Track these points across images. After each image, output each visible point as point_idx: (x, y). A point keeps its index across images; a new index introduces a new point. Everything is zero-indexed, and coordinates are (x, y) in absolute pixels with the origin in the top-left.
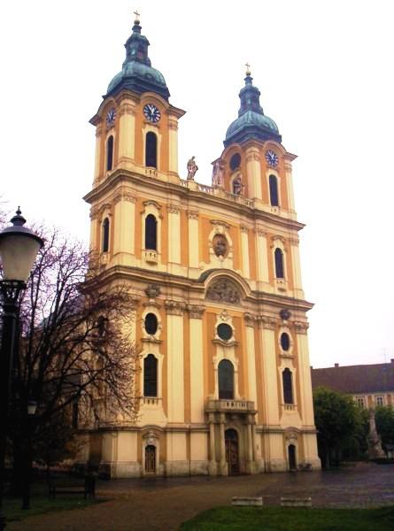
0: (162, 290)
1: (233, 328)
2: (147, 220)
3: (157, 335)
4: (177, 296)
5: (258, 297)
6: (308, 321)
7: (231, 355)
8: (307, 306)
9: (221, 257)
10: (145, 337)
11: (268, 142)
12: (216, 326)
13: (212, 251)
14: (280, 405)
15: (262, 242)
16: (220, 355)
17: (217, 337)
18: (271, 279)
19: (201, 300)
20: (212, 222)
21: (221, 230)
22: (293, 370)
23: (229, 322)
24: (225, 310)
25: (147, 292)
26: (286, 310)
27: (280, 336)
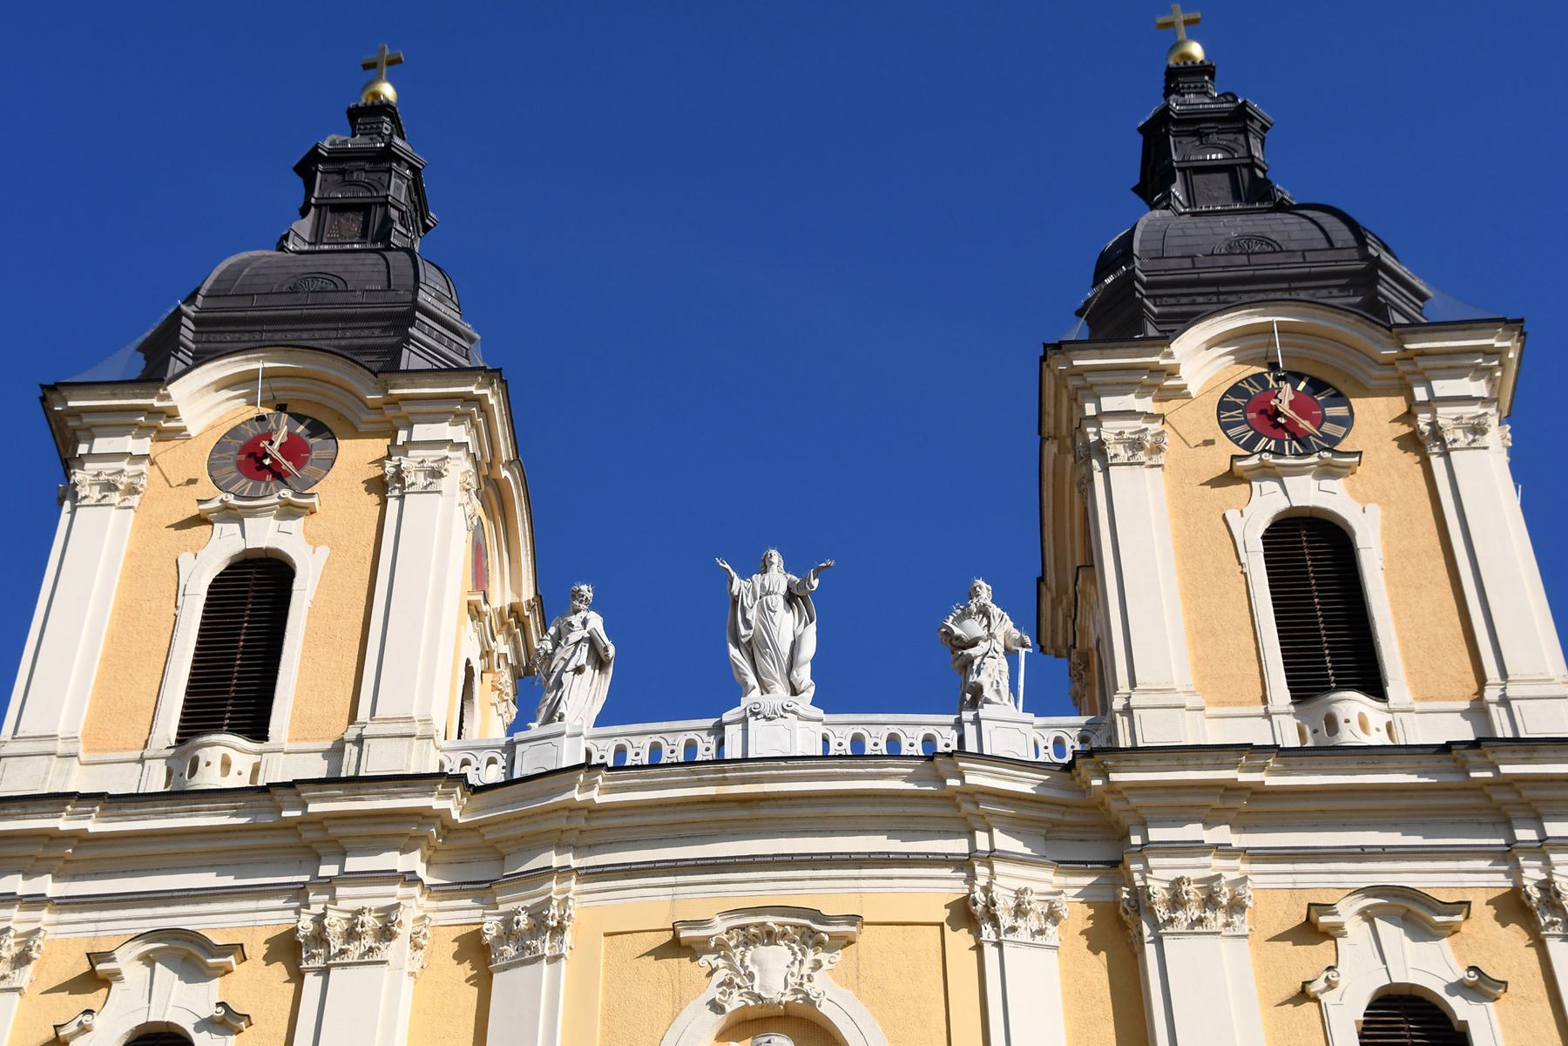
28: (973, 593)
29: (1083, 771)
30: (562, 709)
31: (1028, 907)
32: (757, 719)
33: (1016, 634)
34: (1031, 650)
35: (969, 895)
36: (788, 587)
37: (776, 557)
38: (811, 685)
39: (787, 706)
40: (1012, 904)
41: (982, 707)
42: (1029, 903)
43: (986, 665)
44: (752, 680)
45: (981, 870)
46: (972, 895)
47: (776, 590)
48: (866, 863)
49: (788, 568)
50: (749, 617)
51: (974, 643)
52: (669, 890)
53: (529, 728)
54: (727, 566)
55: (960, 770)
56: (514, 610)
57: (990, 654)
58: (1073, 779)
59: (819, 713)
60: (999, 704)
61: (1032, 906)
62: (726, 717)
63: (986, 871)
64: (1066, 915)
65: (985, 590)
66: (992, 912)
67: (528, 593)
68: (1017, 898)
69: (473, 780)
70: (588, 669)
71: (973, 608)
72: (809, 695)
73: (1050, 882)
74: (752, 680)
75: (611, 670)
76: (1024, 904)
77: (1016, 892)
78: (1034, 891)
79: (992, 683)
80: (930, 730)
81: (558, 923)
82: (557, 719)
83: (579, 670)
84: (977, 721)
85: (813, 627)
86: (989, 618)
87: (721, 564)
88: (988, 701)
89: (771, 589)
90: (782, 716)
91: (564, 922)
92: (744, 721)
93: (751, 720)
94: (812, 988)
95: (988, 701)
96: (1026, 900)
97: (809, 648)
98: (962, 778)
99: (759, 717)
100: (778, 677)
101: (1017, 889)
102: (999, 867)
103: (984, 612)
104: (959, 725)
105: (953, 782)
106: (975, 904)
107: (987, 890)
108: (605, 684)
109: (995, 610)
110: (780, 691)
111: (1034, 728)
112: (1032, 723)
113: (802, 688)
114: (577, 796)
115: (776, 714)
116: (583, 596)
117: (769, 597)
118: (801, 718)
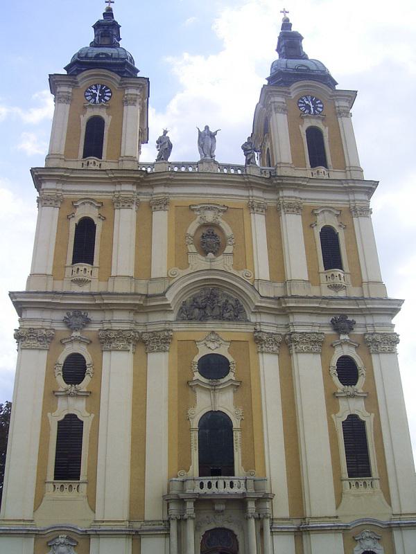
0: (94, 316)
1: (230, 359)
2: (78, 227)
3: (83, 386)
4: (121, 321)
5: (280, 304)
6: (396, 330)
7: (226, 402)
8: (393, 308)
9: (211, 255)
10: (61, 389)
11: (294, 85)
12: (196, 359)
13: (192, 248)
14: (338, 481)
15: (293, 225)
16: (203, 404)
17: (197, 376)
18: (313, 272)
19: (170, 322)
20: (191, 208)
21: (210, 217)
22: (364, 416)
23: (223, 351)
24: (213, 332)
25: (66, 322)
26: (344, 317)
27: (334, 363)
94: (220, 220)
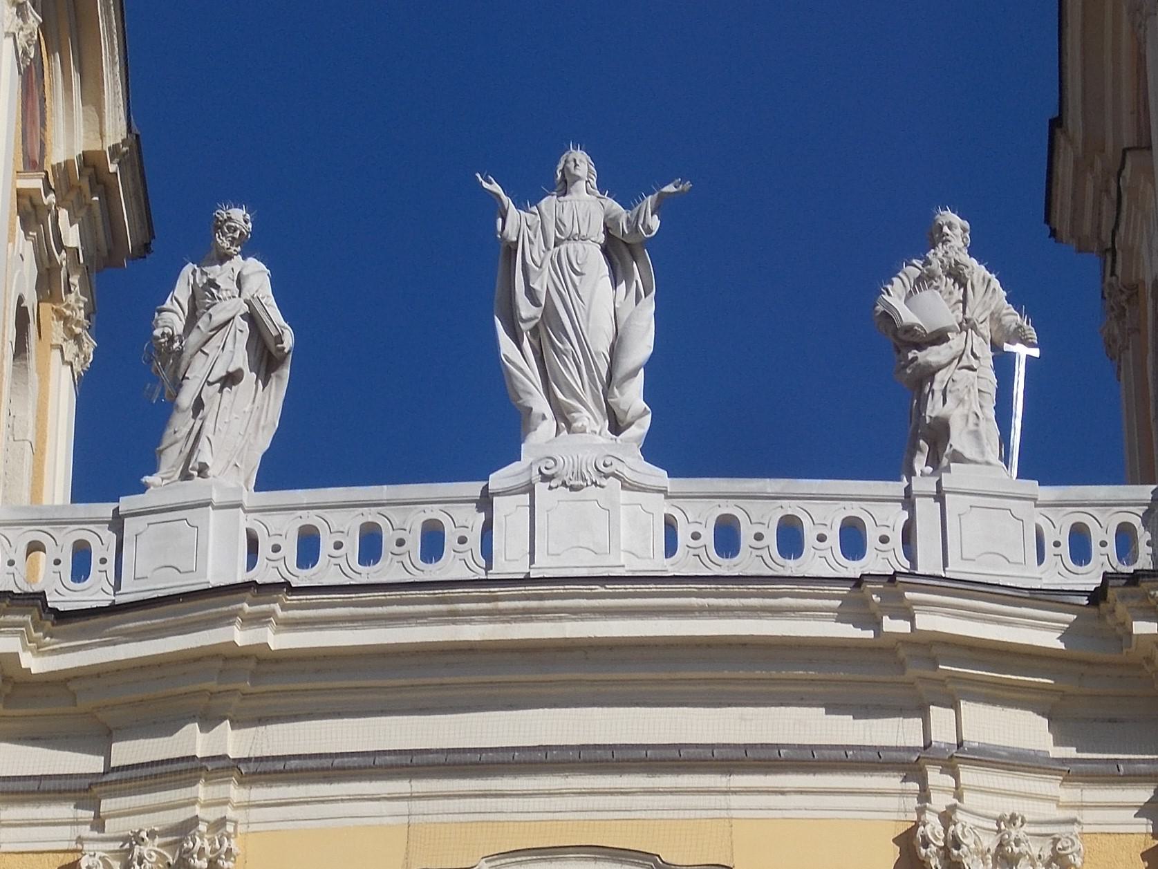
28: (934, 237)
29: (1120, 608)
30: (205, 455)
31: (1016, 850)
32: (550, 488)
33: (1013, 318)
34: (1035, 352)
35: (916, 826)
36: (605, 224)
37: (581, 162)
38: (645, 412)
39: (605, 465)
40: (990, 842)
41: (948, 469)
42: (1017, 842)
43: (958, 386)
44: (539, 403)
45: (935, 777)
46: (921, 828)
47: (583, 233)
48: (737, 766)
49: (607, 185)
50: (535, 285)
51: (940, 337)
52: (402, 806)
53: (143, 488)
54: (496, 188)
55: (906, 604)
56: (90, 162)
57: (964, 362)
58: (1101, 617)
59: (658, 476)
60: (976, 462)
61: (1023, 848)
62: (497, 480)
63: (949, 781)
64: (1078, 861)
65: (959, 231)
66: (953, 859)
67: (115, 130)
68: (999, 831)
69: (53, 601)
70: (250, 377)
71: (936, 265)
72: (640, 429)
73: (1055, 800)
74: (539, 403)
75: (286, 372)
76: (1008, 844)
77: (999, 821)
78: (1027, 818)
79: (967, 417)
80: (854, 510)
81: (210, 861)
82: (195, 473)
83: (231, 379)
84: (940, 497)
85: (648, 307)
86: (963, 285)
87: (486, 185)
88: (958, 458)
89: (576, 230)
90: (595, 484)
91: (220, 862)
92: (530, 489)
93: (541, 488)
95: (958, 458)
96: (1013, 838)
97: (642, 346)
98: (912, 619)
99: (553, 484)
100: (588, 399)
101: (998, 814)
102: (969, 775)
103: (957, 275)
104: (908, 501)
105: (892, 625)
106: (926, 844)
107: (947, 818)
108: (276, 398)
109: (977, 271)
110: (590, 419)
111: (1036, 506)
112: (1035, 500)
113: (629, 418)
114: (241, 636)
115: (584, 480)
116: (235, 230)
117: (571, 245)
118: (627, 486)
